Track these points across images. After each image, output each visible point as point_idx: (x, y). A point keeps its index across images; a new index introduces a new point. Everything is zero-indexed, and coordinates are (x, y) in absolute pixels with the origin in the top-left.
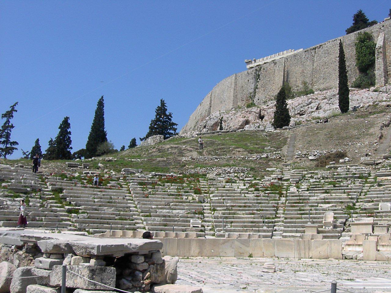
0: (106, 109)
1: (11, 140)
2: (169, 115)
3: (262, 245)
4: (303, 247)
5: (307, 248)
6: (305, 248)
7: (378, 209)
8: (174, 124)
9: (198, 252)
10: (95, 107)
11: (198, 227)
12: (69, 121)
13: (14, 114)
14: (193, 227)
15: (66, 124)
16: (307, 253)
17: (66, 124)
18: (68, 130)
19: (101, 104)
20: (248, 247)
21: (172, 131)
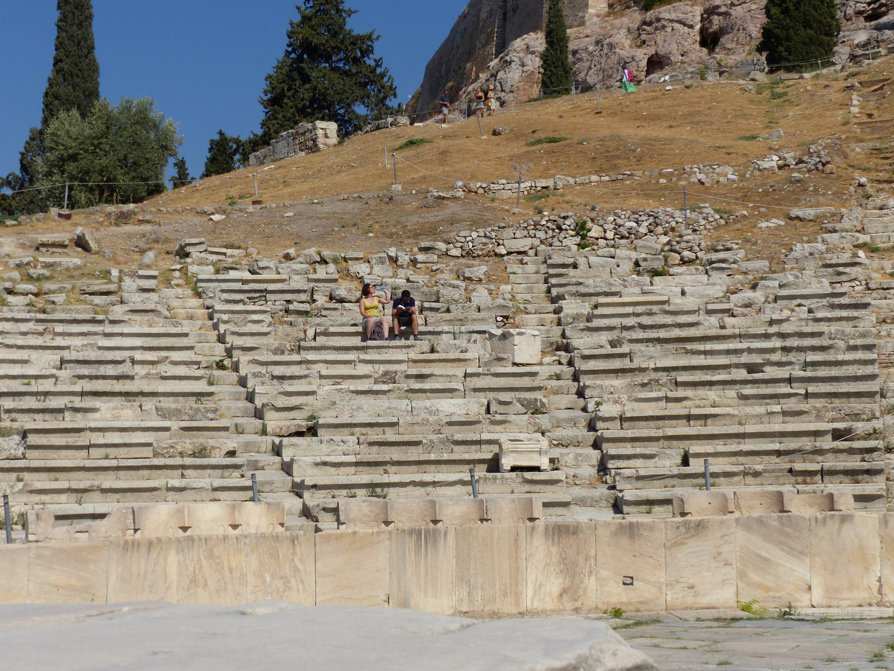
3: (874, 543)
9: (556, 591)
11: (537, 469)
14: (514, 469)
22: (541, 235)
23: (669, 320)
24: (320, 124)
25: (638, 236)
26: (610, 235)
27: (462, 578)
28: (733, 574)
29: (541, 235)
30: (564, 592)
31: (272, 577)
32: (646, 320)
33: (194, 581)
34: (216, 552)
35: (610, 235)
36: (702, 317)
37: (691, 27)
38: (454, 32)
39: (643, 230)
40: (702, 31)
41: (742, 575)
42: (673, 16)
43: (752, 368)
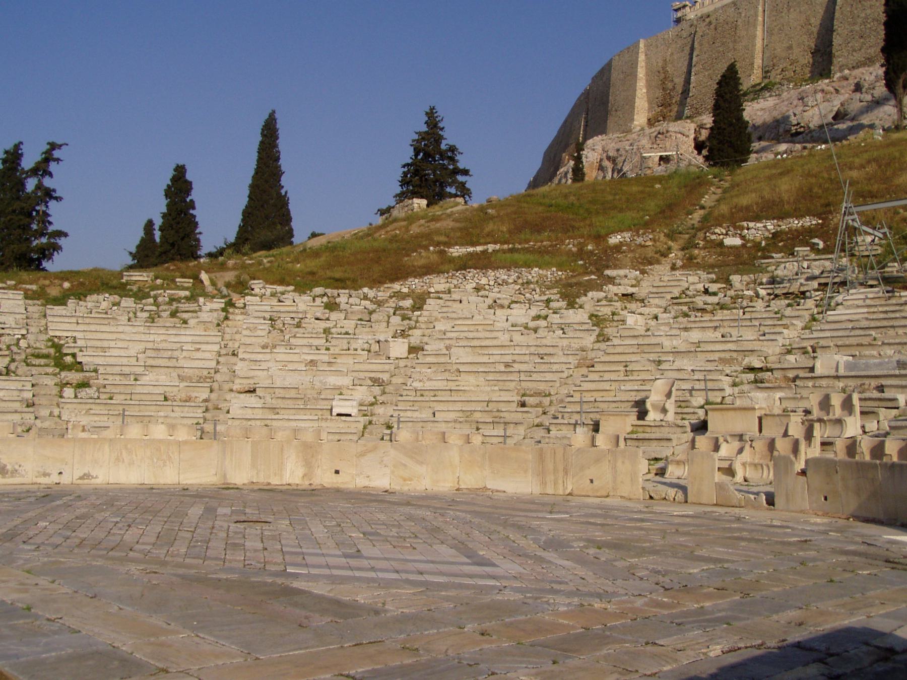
0: (283, 144)
1: (51, 229)
2: (446, 151)
3: (457, 459)
4: (550, 466)
5: (561, 467)
6: (555, 470)
7: (812, 369)
8: (466, 172)
9: (301, 475)
10: (256, 139)
11: (350, 415)
12: (189, 177)
13: (53, 167)
14: (338, 415)
15: (179, 188)
16: (560, 482)
17: (179, 188)
18: (188, 200)
19: (270, 132)
20: (421, 463)
21: (453, 190)
22: (455, 282)
23: (488, 335)
24: (416, 200)
25: (507, 283)
26: (492, 283)
27: (254, 465)
28: (388, 471)
29: (455, 282)
30: (305, 476)
31: (158, 459)
32: (471, 335)
33: (118, 459)
34: (129, 446)
35: (492, 283)
36: (499, 334)
37: (687, 136)
38: (559, 132)
39: (511, 281)
40: (695, 139)
41: (393, 472)
42: (677, 129)
43: (507, 365)
